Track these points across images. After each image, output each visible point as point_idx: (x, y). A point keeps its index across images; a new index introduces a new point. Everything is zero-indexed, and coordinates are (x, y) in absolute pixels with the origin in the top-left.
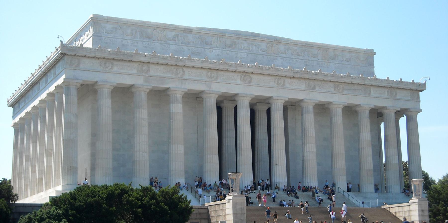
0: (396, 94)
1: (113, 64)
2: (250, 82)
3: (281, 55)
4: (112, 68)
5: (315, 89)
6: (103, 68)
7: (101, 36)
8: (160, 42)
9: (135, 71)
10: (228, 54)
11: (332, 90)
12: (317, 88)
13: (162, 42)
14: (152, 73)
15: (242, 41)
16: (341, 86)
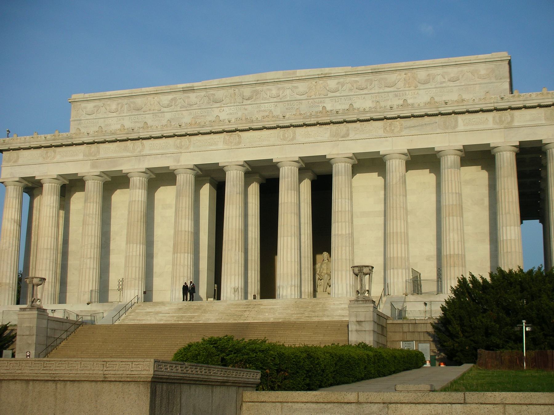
0: (512, 120)
1: (55, 152)
2: (239, 143)
3: (330, 94)
4: (54, 158)
5: (348, 135)
6: (44, 158)
7: (81, 120)
8: (151, 112)
9: (81, 157)
10: (246, 109)
11: (381, 132)
12: (352, 136)
13: (154, 112)
14: (102, 154)
15: (268, 87)
16: (398, 123)
